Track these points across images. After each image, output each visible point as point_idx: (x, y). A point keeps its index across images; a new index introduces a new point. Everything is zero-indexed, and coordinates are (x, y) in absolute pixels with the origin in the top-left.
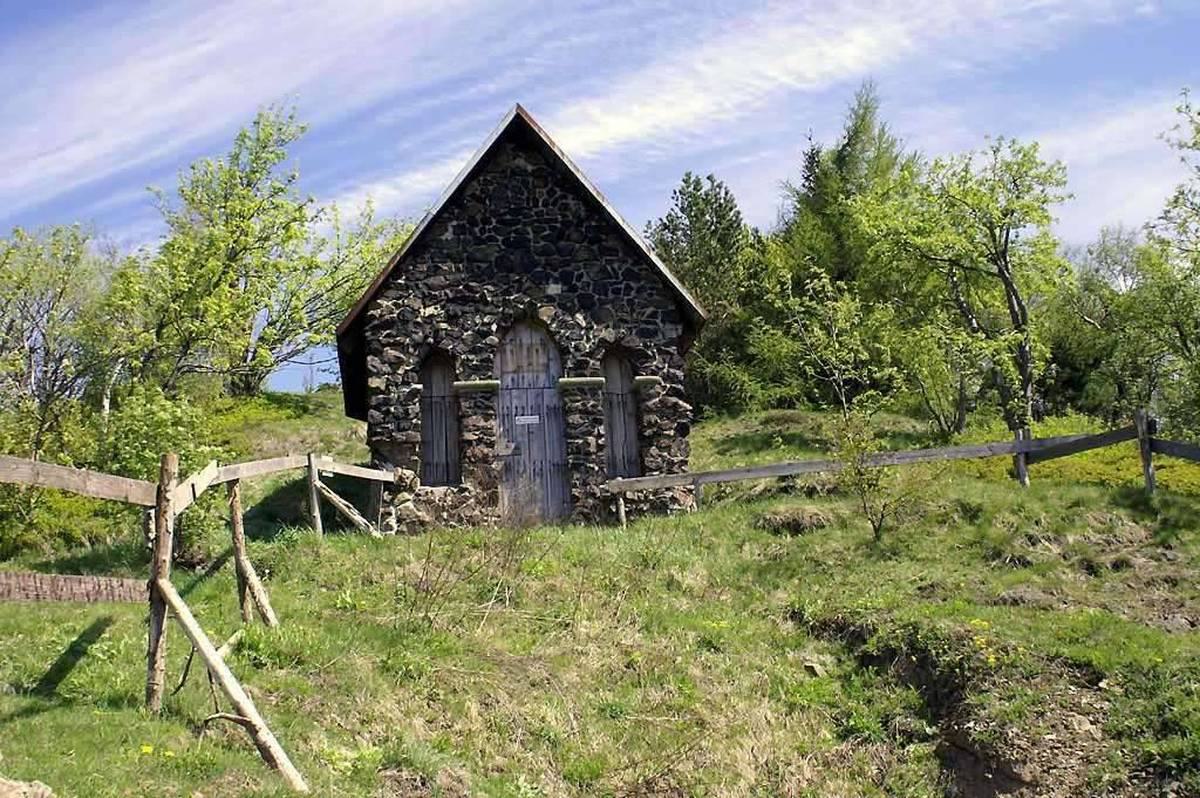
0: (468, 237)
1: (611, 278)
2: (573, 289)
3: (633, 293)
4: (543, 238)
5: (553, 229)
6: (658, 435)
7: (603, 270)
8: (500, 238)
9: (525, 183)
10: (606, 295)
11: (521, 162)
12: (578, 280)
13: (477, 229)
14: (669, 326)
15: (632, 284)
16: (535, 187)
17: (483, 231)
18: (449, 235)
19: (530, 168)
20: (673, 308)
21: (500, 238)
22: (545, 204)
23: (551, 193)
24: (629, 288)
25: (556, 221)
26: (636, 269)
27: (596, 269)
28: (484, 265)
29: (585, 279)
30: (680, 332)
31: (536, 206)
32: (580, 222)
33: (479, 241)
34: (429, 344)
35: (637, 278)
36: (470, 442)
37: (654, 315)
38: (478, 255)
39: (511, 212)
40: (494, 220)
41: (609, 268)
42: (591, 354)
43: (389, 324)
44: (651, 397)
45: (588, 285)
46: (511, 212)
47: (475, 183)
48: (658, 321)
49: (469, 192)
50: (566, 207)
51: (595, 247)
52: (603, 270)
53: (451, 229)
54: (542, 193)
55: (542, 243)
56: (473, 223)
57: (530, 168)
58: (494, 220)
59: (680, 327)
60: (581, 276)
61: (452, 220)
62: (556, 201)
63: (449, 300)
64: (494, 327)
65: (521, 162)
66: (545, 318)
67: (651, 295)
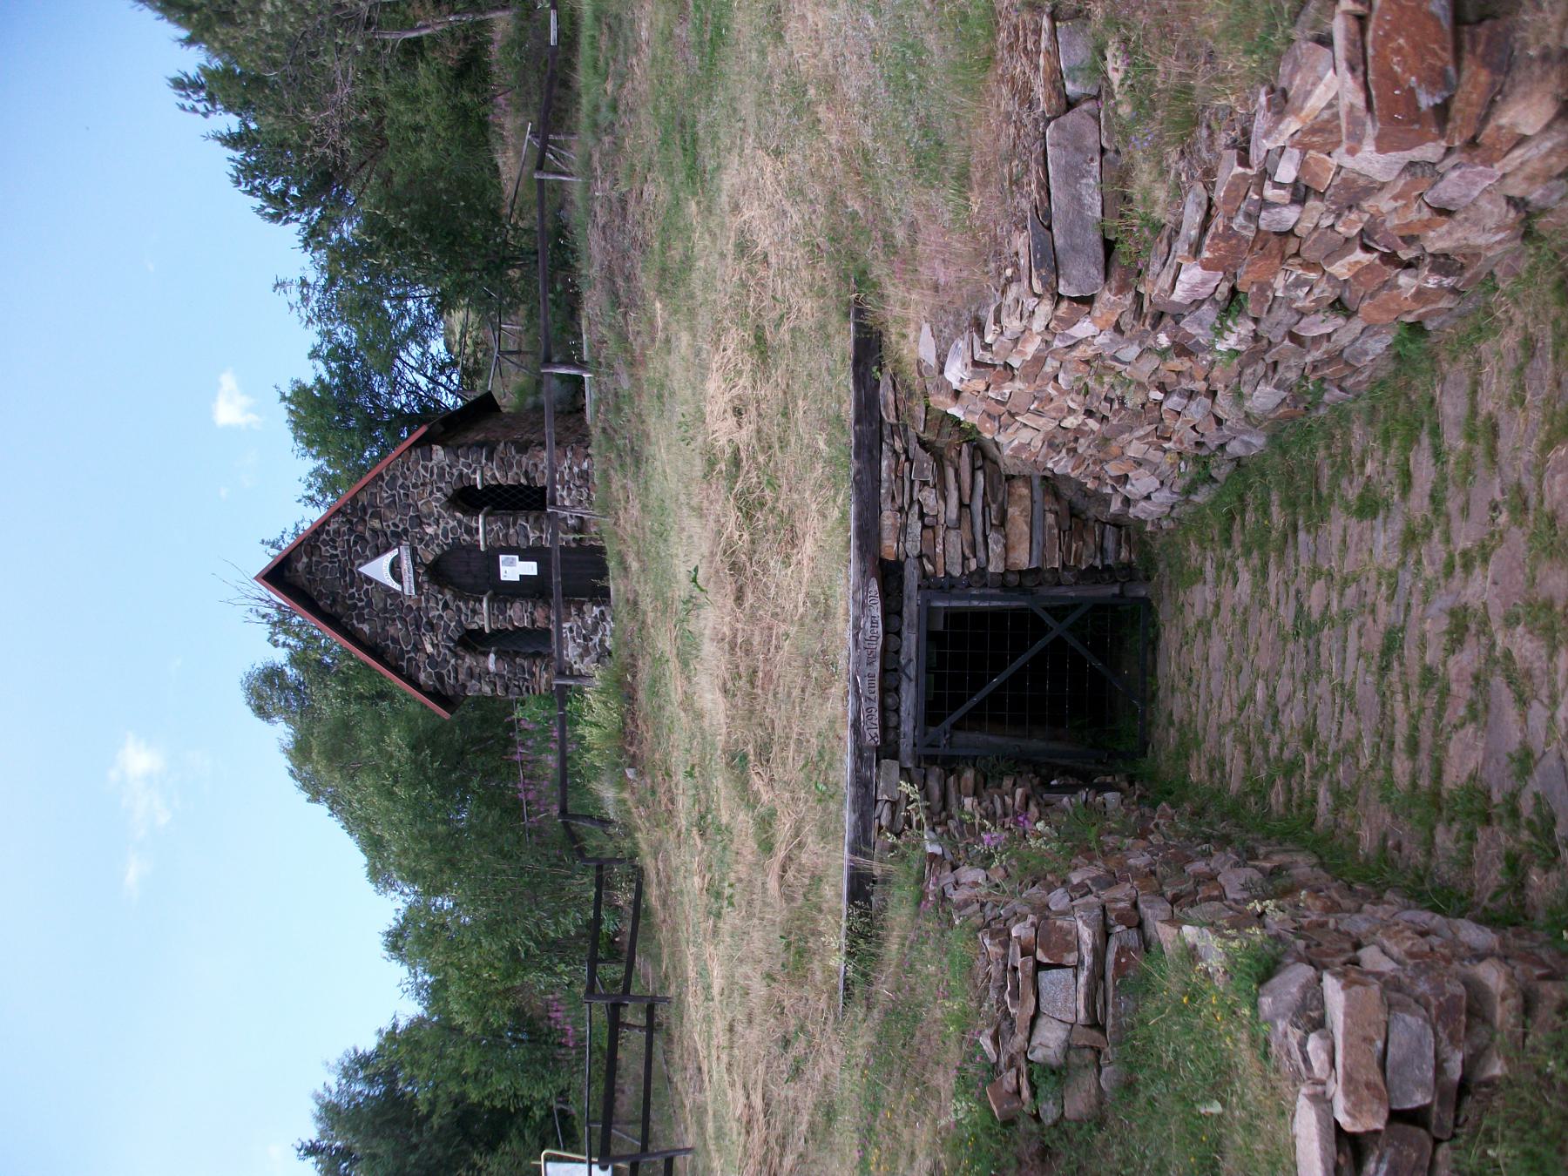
0: (366, 611)
1: (394, 501)
2: (405, 531)
3: (407, 483)
4: (364, 552)
5: (356, 543)
6: (526, 474)
7: (388, 506)
8: (365, 586)
9: (318, 563)
10: (410, 505)
11: (300, 566)
12: (397, 526)
13: (360, 604)
14: (434, 457)
15: (400, 481)
16: (321, 556)
17: (361, 600)
18: (366, 628)
19: (305, 560)
20: (419, 451)
21: (365, 586)
22: (336, 549)
23: (325, 543)
24: (402, 486)
25: (348, 541)
26: (387, 478)
27: (388, 513)
28: (389, 601)
29: (397, 521)
30: (439, 447)
31: (337, 556)
32: (350, 522)
33: (369, 604)
34: (456, 646)
35: (394, 478)
36: (533, 622)
37: (425, 468)
38: (381, 605)
39: (344, 575)
40: (351, 591)
41: (387, 501)
42: (460, 522)
43: (440, 677)
44: (495, 478)
45: (401, 520)
46: (344, 575)
47: (321, 604)
48: (430, 465)
49: (328, 610)
50: (337, 532)
51: (370, 511)
52: (388, 506)
53: (361, 626)
54: (327, 550)
55: (368, 552)
56: (355, 605)
57: (305, 560)
58: (351, 591)
59: (435, 447)
60: (396, 526)
61: (353, 625)
62: (332, 540)
63: (418, 628)
64: (440, 596)
65: (300, 566)
66: (431, 558)
67: (408, 469)
